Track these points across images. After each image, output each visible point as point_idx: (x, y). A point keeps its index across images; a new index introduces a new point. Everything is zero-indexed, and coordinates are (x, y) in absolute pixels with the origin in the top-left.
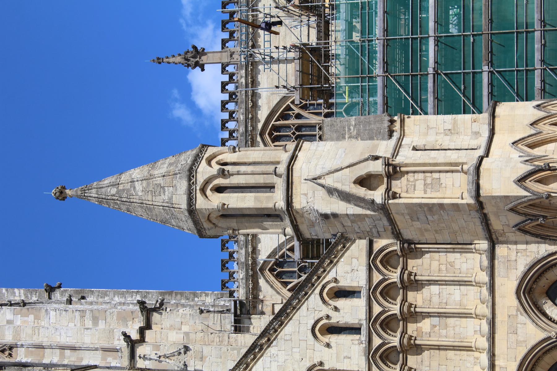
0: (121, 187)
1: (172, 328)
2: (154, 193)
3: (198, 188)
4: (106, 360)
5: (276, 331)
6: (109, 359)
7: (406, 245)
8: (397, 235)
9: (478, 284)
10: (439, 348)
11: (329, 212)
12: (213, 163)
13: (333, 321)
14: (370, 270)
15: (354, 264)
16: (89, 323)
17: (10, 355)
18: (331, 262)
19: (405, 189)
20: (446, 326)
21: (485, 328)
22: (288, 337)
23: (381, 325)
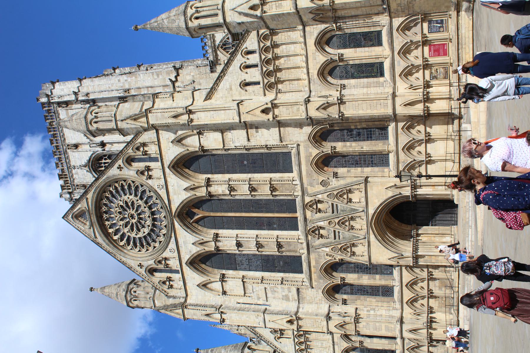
0: (159, 22)
1: (187, 74)
2: (172, 23)
5: (226, 70)
6: (166, 89)
7: (271, 31)
8: (268, 27)
9: (300, 43)
10: (288, 69)
11: (240, 22)
12: (193, 8)
13: (247, 63)
16: (156, 77)
17: (129, 93)
18: (244, 41)
19: (268, 9)
20: (290, 60)
21: (304, 59)
22: (231, 72)
23: (265, 63)
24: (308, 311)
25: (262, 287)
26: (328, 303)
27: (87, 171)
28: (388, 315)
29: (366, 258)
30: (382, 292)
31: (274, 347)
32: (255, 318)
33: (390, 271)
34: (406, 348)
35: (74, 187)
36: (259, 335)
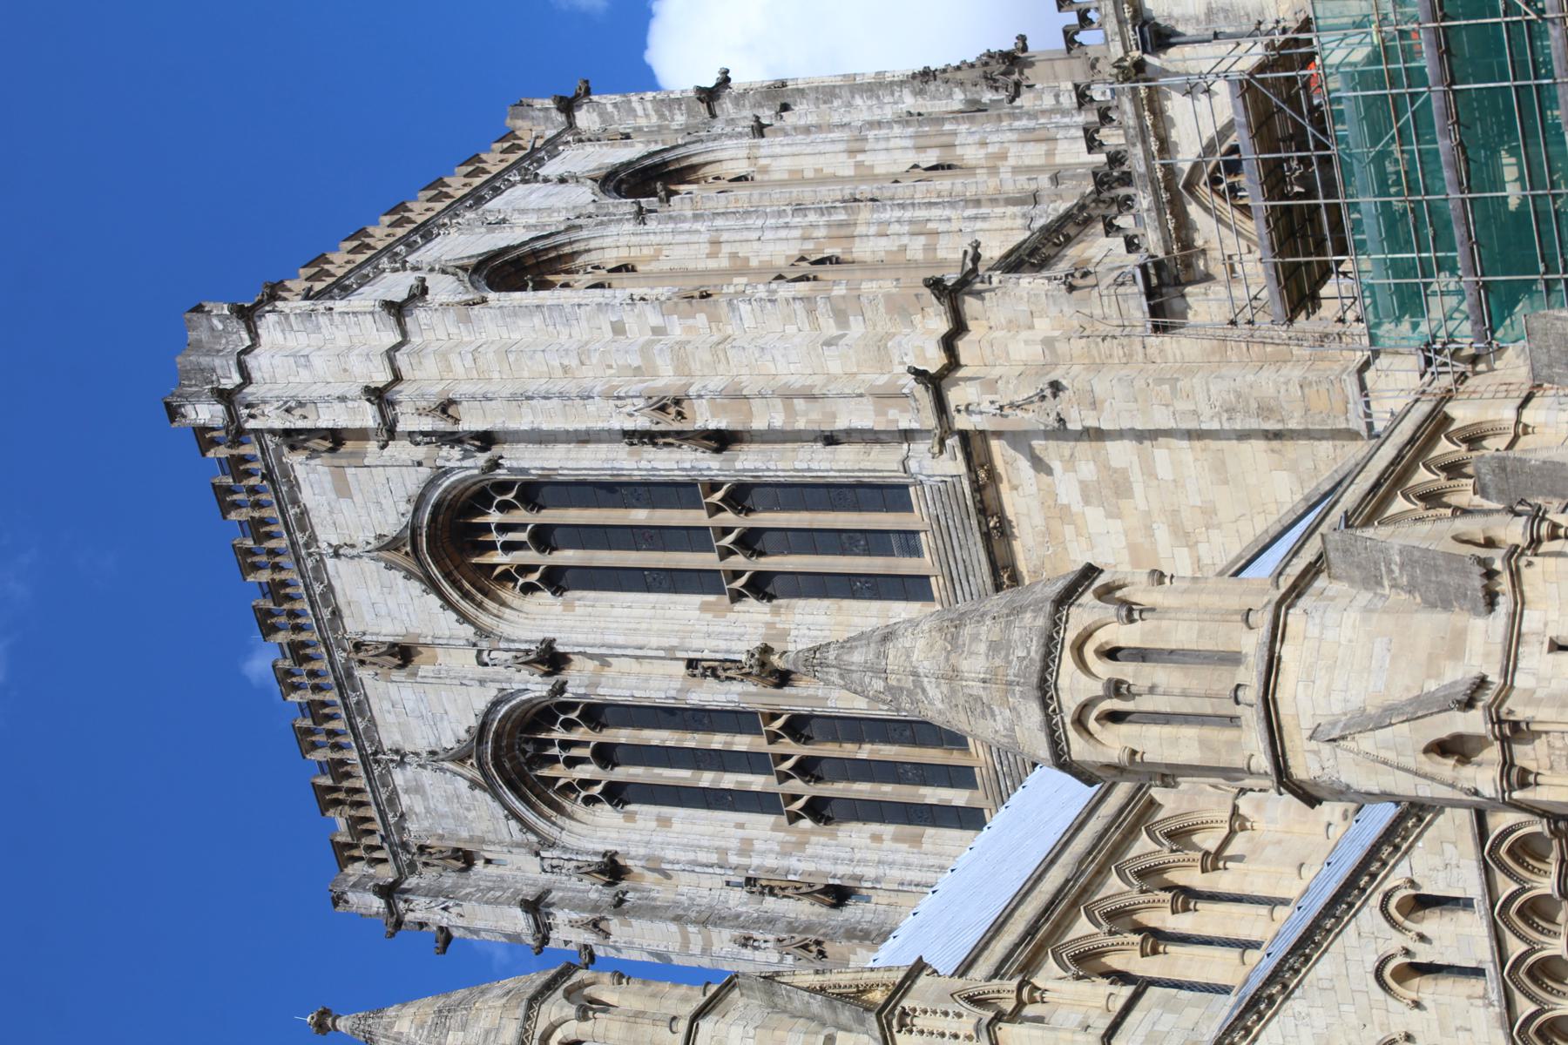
1: (1013, 325)
3: (1068, 720)
4: (885, 414)
5: (1297, 971)
6: (893, 413)
14: (1487, 869)
15: (1448, 855)
16: (830, 328)
19: (1545, 762)
22: (1326, 984)
23: (1530, 973)
27: (474, 784)
35: (405, 857)
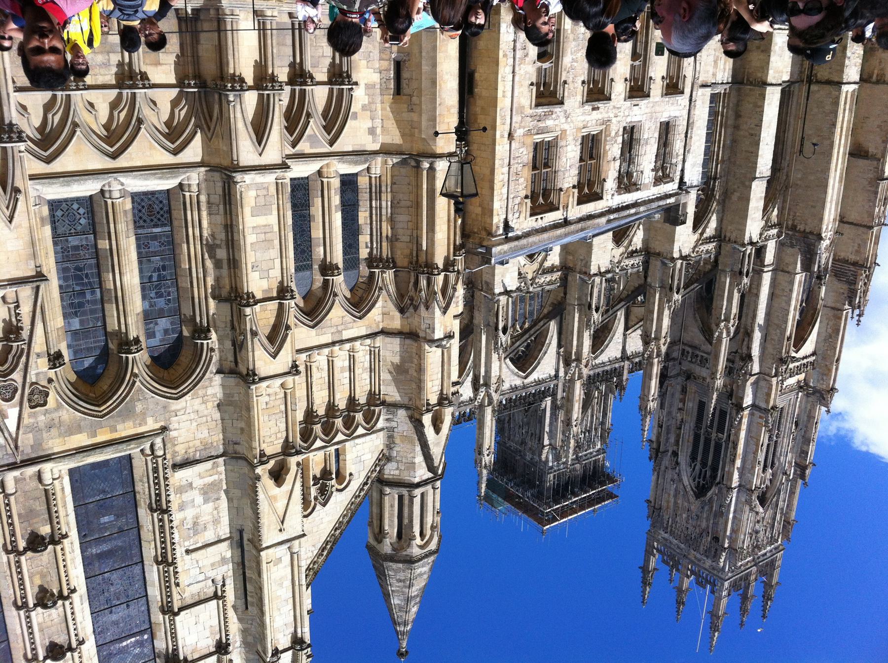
24: (242, 429)
25: (184, 563)
26: (211, 379)
28: (221, 207)
29: (26, 292)
30: (156, 226)
31: (366, 488)
32: (280, 566)
33: (75, 206)
34: (327, 149)
36: (338, 532)
